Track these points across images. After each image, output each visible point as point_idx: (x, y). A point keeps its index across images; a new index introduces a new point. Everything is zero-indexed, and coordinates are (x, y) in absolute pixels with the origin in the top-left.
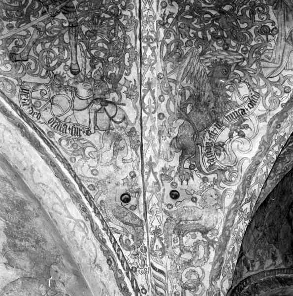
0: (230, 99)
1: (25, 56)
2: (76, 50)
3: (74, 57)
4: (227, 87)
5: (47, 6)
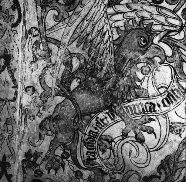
0: (138, 83)
4: (139, 66)
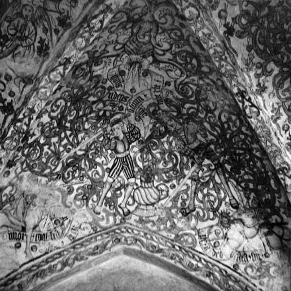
5: (192, 157)
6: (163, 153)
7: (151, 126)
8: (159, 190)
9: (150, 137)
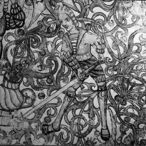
1: (56, 126)
2: (106, 115)
3: (104, 124)
5: (76, 70)
6: (42, 54)
7: (41, 17)
8: (23, 96)
9: (35, 31)
